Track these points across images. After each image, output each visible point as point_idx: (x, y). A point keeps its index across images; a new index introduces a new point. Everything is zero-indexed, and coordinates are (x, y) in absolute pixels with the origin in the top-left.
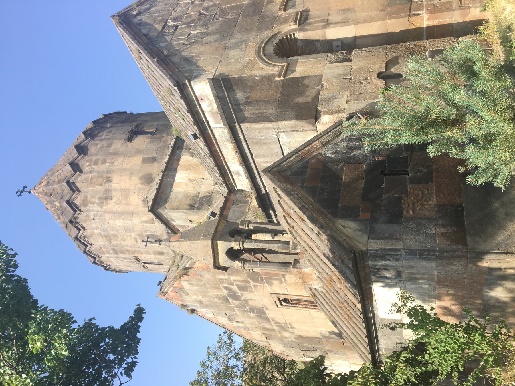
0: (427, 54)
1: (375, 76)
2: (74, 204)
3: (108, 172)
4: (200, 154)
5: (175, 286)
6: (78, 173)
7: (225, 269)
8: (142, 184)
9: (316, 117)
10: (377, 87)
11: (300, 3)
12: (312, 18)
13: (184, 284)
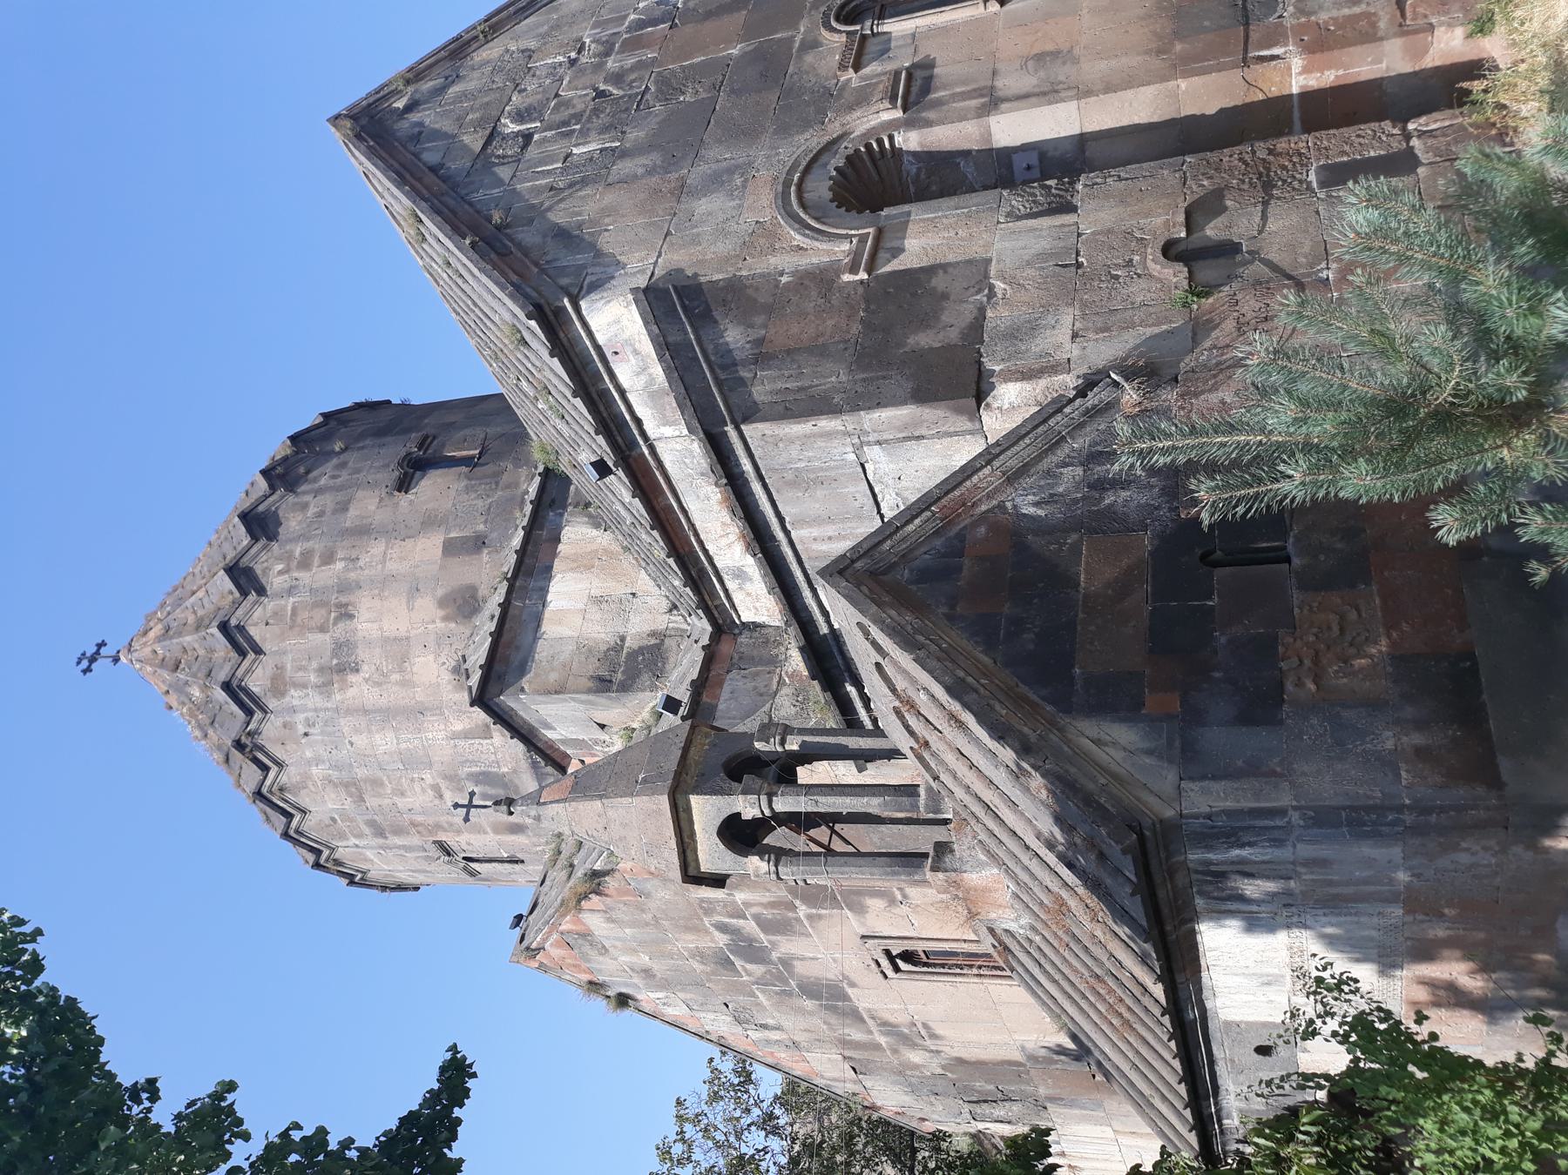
0: (1312, 177)
1: (1153, 252)
3: (344, 587)
4: (619, 521)
5: (563, 928)
6: (253, 596)
7: (718, 881)
8: (446, 619)
9: (979, 391)
10: (1164, 286)
11: (901, 42)
12: (944, 87)
13: (593, 919)
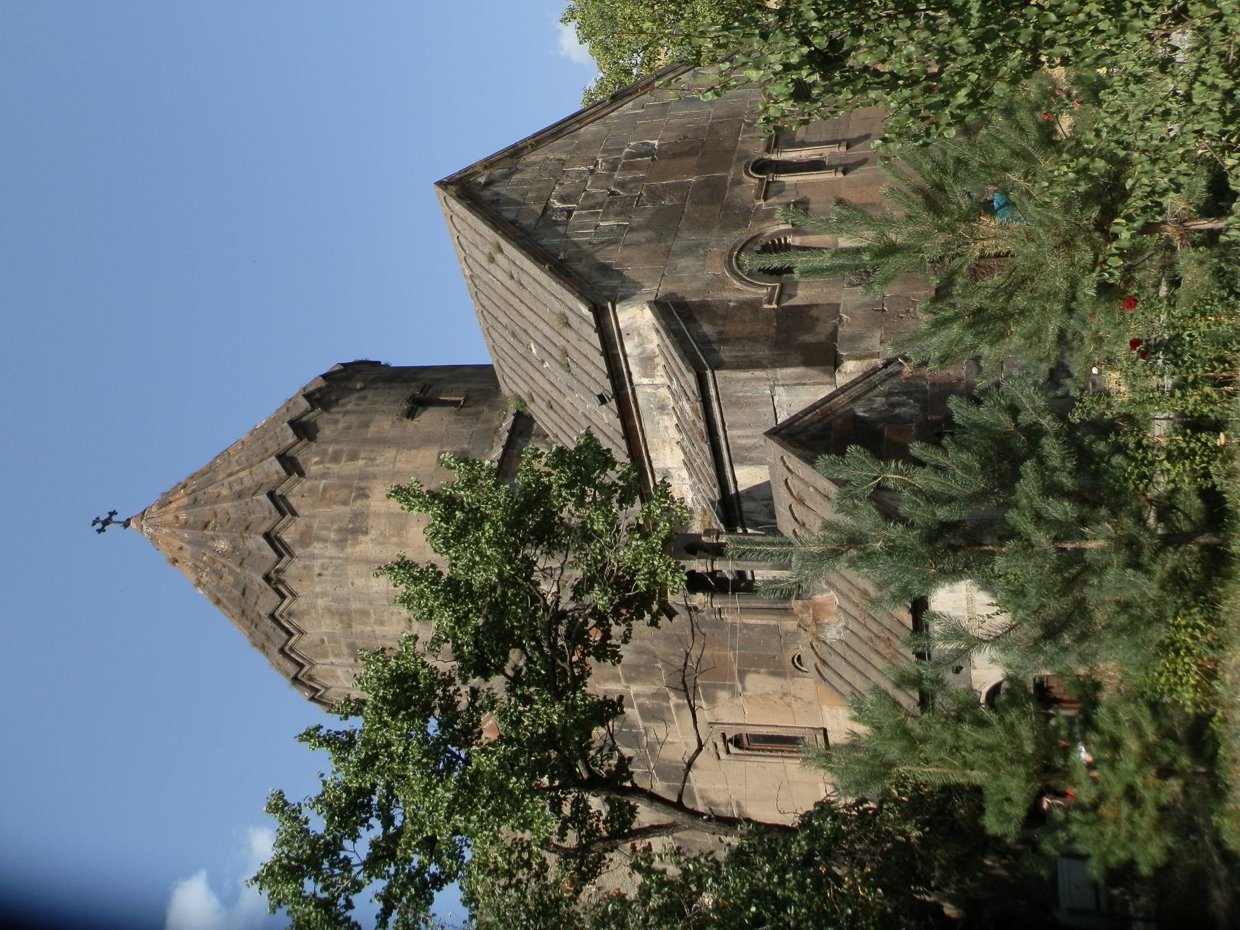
2: (280, 540)
3: (363, 477)
